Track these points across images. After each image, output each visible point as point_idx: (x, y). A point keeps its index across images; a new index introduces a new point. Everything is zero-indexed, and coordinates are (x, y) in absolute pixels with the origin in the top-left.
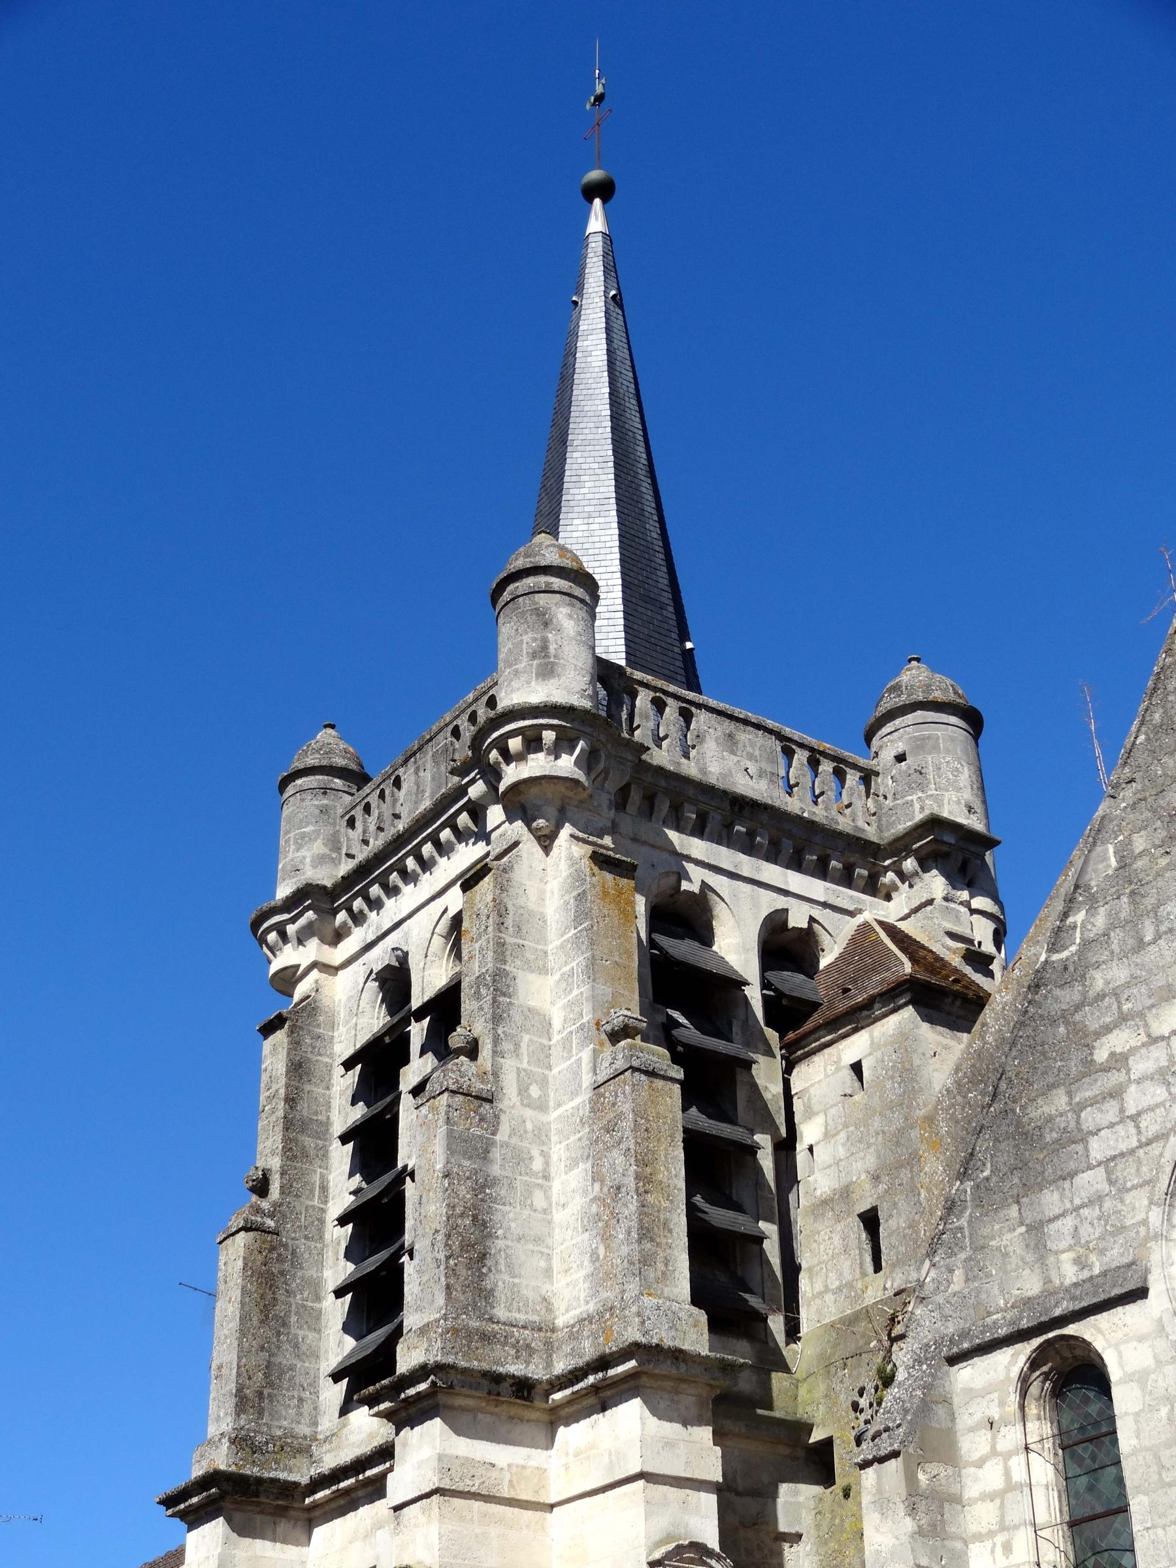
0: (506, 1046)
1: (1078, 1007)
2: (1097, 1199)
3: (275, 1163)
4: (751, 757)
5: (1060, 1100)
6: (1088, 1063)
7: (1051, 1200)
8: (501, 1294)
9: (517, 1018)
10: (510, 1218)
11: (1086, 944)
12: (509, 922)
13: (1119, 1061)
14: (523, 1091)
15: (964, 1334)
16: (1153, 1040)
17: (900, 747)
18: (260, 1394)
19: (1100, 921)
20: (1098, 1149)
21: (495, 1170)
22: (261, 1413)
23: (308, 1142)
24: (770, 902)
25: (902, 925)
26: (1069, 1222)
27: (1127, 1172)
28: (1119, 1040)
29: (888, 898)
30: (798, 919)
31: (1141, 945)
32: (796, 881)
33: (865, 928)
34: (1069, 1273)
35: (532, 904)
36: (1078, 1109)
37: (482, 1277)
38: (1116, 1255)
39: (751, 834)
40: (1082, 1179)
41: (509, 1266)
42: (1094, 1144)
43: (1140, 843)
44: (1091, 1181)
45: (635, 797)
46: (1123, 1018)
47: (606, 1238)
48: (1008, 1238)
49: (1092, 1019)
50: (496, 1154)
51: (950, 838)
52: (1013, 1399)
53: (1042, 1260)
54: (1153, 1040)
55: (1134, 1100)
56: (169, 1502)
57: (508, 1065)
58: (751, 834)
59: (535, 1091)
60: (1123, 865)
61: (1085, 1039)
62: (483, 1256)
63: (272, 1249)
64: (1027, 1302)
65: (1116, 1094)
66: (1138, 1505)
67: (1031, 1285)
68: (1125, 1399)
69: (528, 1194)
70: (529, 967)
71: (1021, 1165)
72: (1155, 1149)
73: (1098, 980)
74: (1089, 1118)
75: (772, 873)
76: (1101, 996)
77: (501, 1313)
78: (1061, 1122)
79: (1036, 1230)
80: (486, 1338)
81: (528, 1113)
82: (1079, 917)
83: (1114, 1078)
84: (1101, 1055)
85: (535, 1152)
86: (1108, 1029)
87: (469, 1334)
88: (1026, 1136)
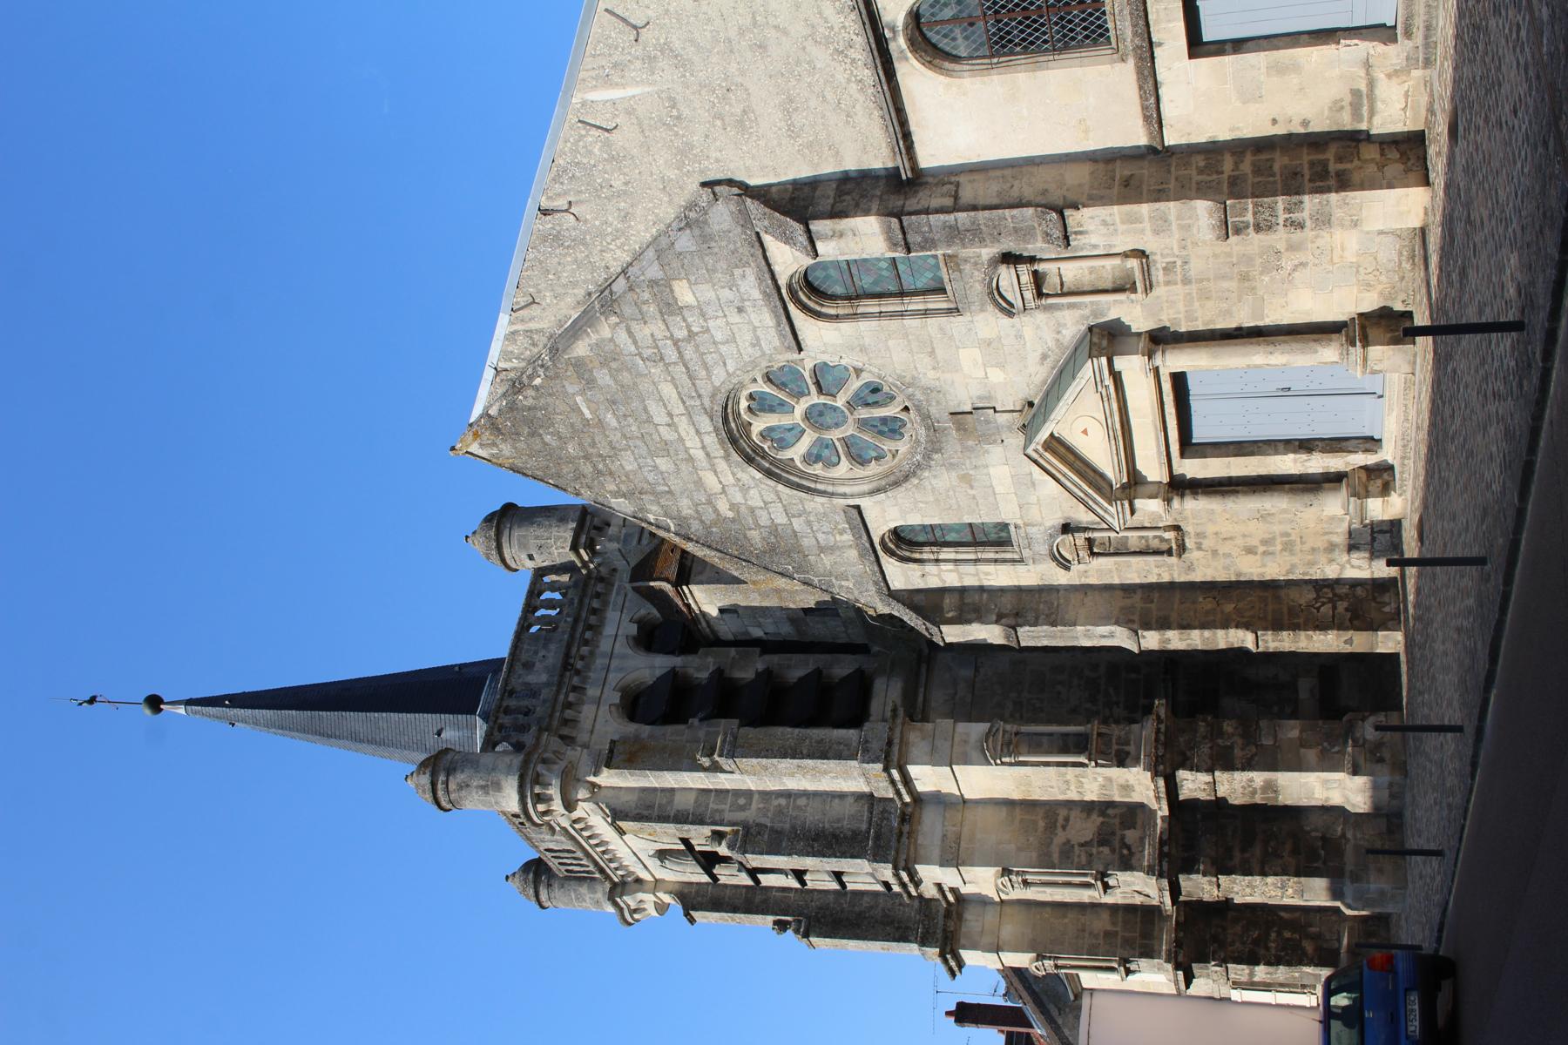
0: (717, 818)
1: (702, 522)
2: (809, 523)
3: (770, 918)
4: (536, 653)
5: (754, 535)
6: (733, 520)
7: (807, 542)
8: (855, 826)
9: (701, 810)
10: (812, 816)
11: (666, 515)
12: (645, 813)
13: (733, 507)
14: (742, 808)
15: (876, 583)
16: (724, 491)
17: (524, 556)
18: (898, 929)
19: (654, 508)
20: (781, 519)
21: (787, 826)
22: (907, 928)
23: (758, 899)
24: (621, 647)
25: (633, 564)
26: (821, 536)
27: (794, 510)
28: (723, 507)
29: (615, 570)
30: (633, 629)
31: (670, 492)
32: (609, 630)
33: (635, 589)
34: (848, 537)
35: (633, 798)
36: (758, 526)
37: (845, 837)
38: (840, 518)
39: (582, 658)
40: (796, 527)
41: (839, 820)
42: (777, 521)
43: (612, 487)
44: (797, 524)
45: (565, 731)
46: (710, 503)
47: (826, 773)
48: (827, 561)
49: (709, 516)
50: (778, 826)
51: (583, 539)
52: (912, 565)
53: (838, 548)
54: (724, 491)
55: (755, 501)
56: (953, 975)
57: (728, 816)
58: (582, 658)
59: (742, 801)
60: (624, 496)
61: (720, 519)
62: (834, 836)
63: (819, 921)
64: (861, 556)
65: (752, 510)
66: (967, 519)
67: (853, 554)
68: (914, 519)
69: (799, 808)
70: (671, 802)
71: (788, 553)
72: (784, 497)
73: (687, 512)
74: (764, 521)
75: (605, 645)
76: (697, 512)
77: (864, 827)
78: (765, 535)
79: (822, 549)
80: (878, 837)
81: (754, 806)
82: (651, 518)
83: (743, 509)
84: (730, 514)
85: (775, 803)
86: (716, 511)
87: (877, 846)
88: (772, 549)
